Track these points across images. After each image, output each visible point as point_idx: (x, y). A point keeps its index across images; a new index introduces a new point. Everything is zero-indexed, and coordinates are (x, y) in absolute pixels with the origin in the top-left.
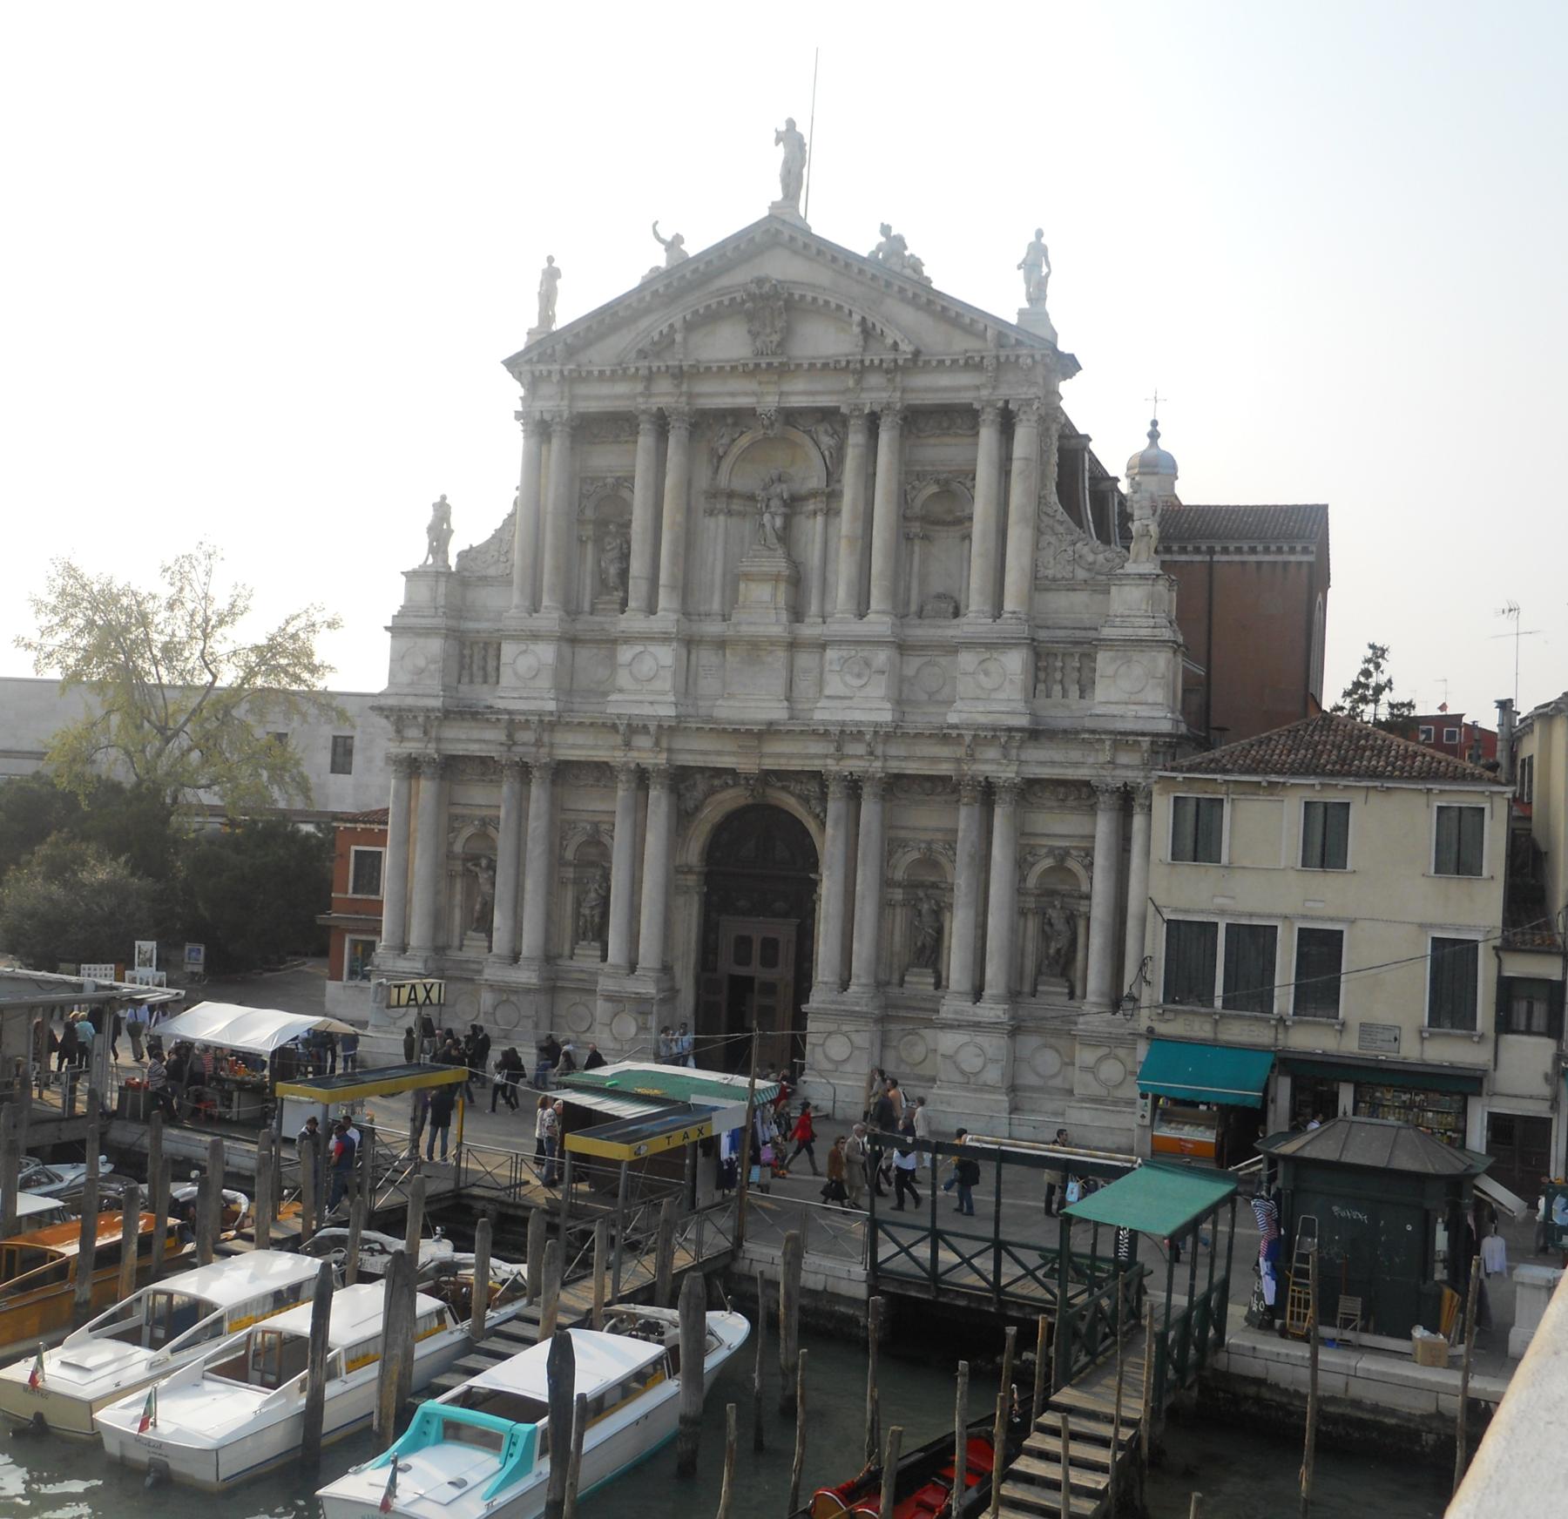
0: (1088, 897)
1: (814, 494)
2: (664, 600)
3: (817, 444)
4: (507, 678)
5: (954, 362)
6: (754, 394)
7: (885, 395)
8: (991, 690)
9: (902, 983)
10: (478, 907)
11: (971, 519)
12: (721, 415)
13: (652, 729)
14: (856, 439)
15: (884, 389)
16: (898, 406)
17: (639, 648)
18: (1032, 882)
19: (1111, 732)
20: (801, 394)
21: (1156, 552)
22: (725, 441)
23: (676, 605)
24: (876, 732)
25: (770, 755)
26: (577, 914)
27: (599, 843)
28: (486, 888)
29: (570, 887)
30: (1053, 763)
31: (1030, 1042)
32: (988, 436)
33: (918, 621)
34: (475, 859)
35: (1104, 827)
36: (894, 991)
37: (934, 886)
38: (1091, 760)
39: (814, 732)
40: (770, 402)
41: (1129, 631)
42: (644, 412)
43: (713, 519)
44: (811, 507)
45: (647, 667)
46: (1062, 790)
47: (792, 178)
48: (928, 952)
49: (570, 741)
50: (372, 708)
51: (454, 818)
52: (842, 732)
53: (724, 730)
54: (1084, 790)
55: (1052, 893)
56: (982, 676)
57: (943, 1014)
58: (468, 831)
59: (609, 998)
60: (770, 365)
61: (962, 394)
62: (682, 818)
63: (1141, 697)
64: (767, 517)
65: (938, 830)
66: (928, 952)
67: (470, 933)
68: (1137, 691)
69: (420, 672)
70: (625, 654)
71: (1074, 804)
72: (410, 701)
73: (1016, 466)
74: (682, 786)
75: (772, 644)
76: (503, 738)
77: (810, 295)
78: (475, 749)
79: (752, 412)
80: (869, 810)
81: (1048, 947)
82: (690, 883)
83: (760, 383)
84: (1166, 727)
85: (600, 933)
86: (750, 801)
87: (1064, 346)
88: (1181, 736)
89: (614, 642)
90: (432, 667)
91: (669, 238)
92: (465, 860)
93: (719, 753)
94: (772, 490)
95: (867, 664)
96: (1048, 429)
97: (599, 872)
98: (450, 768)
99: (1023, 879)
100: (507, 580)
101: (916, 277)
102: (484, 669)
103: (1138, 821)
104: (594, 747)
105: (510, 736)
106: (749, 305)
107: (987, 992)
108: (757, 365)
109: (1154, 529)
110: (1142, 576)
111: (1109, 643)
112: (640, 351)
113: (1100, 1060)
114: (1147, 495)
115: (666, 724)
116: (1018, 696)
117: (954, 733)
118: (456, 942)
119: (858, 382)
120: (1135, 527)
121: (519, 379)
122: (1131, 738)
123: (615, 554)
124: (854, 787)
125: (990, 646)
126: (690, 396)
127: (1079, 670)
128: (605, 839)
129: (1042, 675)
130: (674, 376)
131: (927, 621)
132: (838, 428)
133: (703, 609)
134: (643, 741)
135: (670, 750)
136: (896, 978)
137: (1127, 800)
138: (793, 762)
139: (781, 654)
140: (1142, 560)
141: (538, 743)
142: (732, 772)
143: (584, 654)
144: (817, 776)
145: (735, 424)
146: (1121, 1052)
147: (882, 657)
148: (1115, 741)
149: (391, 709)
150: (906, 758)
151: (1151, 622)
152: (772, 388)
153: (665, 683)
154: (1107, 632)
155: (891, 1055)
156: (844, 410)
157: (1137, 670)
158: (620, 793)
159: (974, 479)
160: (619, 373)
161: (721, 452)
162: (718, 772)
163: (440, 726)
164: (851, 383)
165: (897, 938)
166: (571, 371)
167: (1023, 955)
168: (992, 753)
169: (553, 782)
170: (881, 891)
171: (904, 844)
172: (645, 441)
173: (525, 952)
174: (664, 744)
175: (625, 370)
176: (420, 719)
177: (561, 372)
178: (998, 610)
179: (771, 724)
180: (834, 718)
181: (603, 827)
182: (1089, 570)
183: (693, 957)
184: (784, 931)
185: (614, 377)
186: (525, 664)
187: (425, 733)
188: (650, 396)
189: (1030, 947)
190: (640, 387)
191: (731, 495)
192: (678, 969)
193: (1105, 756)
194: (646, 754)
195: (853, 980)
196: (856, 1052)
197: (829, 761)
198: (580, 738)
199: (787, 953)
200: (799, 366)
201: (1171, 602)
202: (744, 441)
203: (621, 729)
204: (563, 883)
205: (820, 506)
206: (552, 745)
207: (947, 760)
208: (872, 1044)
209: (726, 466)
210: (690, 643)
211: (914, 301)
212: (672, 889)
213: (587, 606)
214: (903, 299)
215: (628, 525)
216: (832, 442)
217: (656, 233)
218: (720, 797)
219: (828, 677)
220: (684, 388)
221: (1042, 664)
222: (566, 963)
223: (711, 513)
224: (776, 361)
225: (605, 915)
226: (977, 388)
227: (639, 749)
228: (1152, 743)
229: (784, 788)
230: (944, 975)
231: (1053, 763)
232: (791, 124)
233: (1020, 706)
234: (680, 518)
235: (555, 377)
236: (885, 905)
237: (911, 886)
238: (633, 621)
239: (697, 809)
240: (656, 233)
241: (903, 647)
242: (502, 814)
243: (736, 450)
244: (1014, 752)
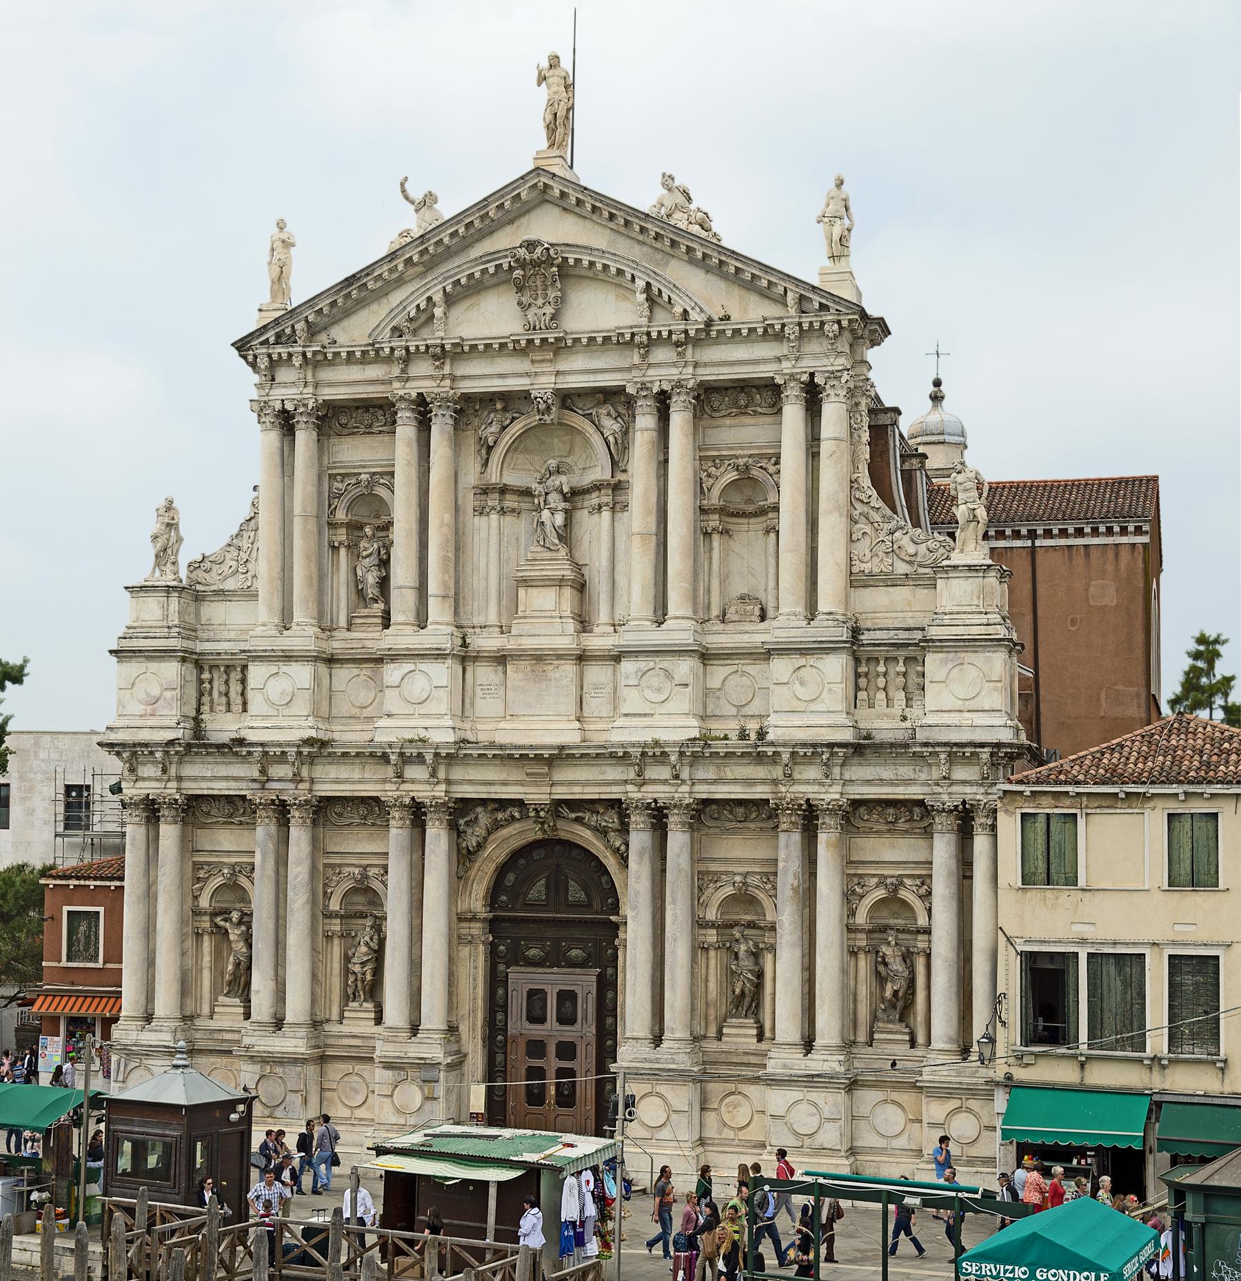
0: (927, 931)
1: (597, 487)
3: (598, 428)
4: (256, 702)
6: (528, 375)
7: (674, 371)
8: (808, 702)
9: (720, 1036)
10: (230, 967)
11: (776, 509)
12: (488, 400)
13: (429, 758)
14: (645, 421)
15: (674, 364)
16: (691, 384)
17: (407, 667)
18: (861, 918)
19: (946, 744)
20: (581, 372)
21: (986, 537)
22: (494, 428)
23: (448, 617)
24: (682, 754)
25: (562, 783)
26: (346, 972)
27: (369, 890)
28: (240, 946)
29: (336, 941)
30: (882, 782)
31: (868, 1098)
32: (793, 413)
33: (720, 627)
34: (225, 913)
35: (943, 849)
36: (711, 1046)
37: (752, 925)
38: (923, 776)
39: (613, 756)
40: (544, 383)
41: (955, 630)
42: (402, 398)
43: (485, 518)
44: (595, 502)
46: (891, 811)
47: (559, 125)
48: (747, 1000)
49: (332, 775)
50: (99, 744)
51: (197, 866)
52: (643, 754)
53: (510, 757)
54: (917, 810)
55: (884, 929)
57: (769, 1070)
58: (217, 881)
59: (388, 1066)
61: (761, 368)
62: (463, 857)
63: (972, 705)
64: (546, 514)
65: (754, 861)
66: (747, 1000)
67: (221, 999)
68: (970, 698)
70: (392, 673)
71: (906, 826)
73: (825, 448)
74: (462, 822)
75: (559, 657)
76: (256, 774)
78: (220, 788)
79: (525, 396)
80: (678, 840)
81: (883, 989)
82: (475, 932)
83: (533, 362)
84: (1006, 736)
85: (374, 990)
86: (540, 836)
87: (872, 311)
88: (1020, 746)
89: (379, 660)
90: (168, 694)
91: (418, 195)
92: (214, 914)
93: (505, 783)
94: (549, 482)
95: (669, 675)
96: (857, 404)
97: (369, 922)
98: (194, 809)
99: (852, 913)
100: (250, 595)
101: (703, 234)
102: (227, 695)
103: (981, 843)
105: (263, 771)
106: (518, 273)
107: (818, 1042)
108: (530, 342)
109: (982, 513)
110: (970, 568)
111: (940, 645)
112: (394, 329)
113: (951, 1114)
114: (973, 475)
115: (443, 752)
116: (841, 706)
117: (770, 750)
118: (206, 1010)
119: (644, 357)
120: (961, 512)
121: (253, 365)
122: (968, 750)
123: (374, 560)
124: (658, 816)
125: (803, 651)
126: (454, 378)
127: (905, 675)
128: (376, 885)
129: (863, 682)
130: (435, 357)
131: (730, 627)
132: (622, 410)
133: (477, 620)
134: (412, 772)
135: (448, 782)
136: (712, 1032)
137: (965, 818)
139: (569, 669)
140: (972, 551)
141: (297, 779)
142: (520, 803)
143: (343, 674)
144: (615, 804)
145: (505, 409)
146: (974, 1104)
148: (950, 754)
149: (123, 745)
150: (715, 782)
151: (983, 619)
152: (547, 367)
153: (442, 704)
154: (934, 632)
155: (711, 1117)
156: (631, 390)
157: (971, 673)
158: (393, 831)
159: (777, 463)
160: (371, 355)
161: (491, 441)
162: (503, 804)
163: (180, 763)
164: (636, 359)
165: (712, 985)
166: (315, 353)
167: (855, 1001)
168: (813, 772)
169: (314, 823)
170: (692, 933)
171: (716, 877)
172: (406, 431)
173: (289, 1018)
174: (442, 774)
175: (377, 351)
177: (304, 354)
178: (812, 610)
179: (562, 748)
180: (634, 739)
181: (372, 872)
182: (910, 563)
183: (480, 1015)
184: (585, 983)
185: (364, 360)
187: (164, 771)
188: (408, 380)
189: (863, 991)
190: (396, 371)
191: (504, 490)
192: (464, 1028)
193: (936, 774)
194: (420, 785)
195: (667, 1035)
196: (674, 1117)
197: (630, 788)
198: (342, 771)
199: (587, 1006)
200: (577, 341)
201: (1002, 596)
202: (516, 429)
203: (393, 758)
204: (329, 938)
205: (605, 499)
206: (312, 781)
207: (764, 782)
208: (691, 1104)
210: (465, 657)
211: (703, 263)
212: (455, 940)
213: (343, 622)
214: (692, 261)
215: (388, 526)
216: (616, 427)
218: (505, 832)
219: (624, 692)
220: (447, 370)
221: (863, 669)
222: (333, 1028)
223: (481, 511)
224: (551, 337)
225: (378, 971)
226: (779, 360)
227: (413, 781)
228: (992, 755)
229: (579, 820)
230: (767, 1026)
231: (882, 782)
232: (554, 62)
233: (842, 719)
234: (448, 518)
235: (297, 361)
236: (699, 949)
237: (725, 926)
238: (401, 636)
239: (480, 846)
240: (403, 191)
241: (706, 656)
242: (258, 860)
243: (507, 439)
244: (836, 770)
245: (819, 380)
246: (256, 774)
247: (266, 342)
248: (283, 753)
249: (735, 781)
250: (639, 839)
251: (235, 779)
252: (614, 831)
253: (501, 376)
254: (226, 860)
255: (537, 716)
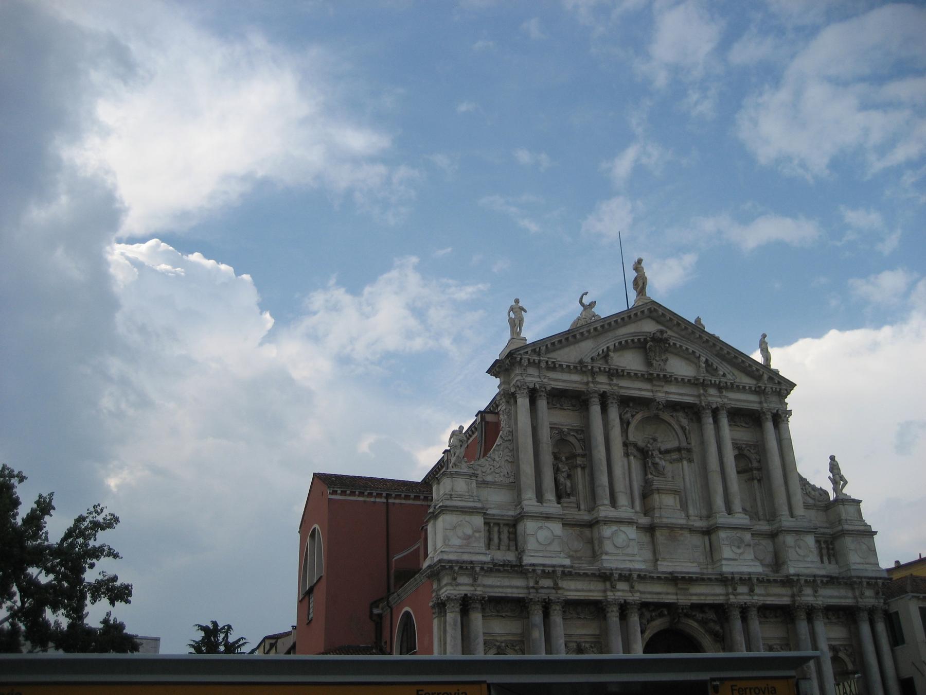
2: (623, 500)
3: (678, 422)
5: (750, 388)
6: (652, 391)
17: (614, 528)
20: (675, 393)
42: (596, 392)
45: (620, 539)
56: (797, 549)
60: (665, 376)
69: (468, 538)
70: (607, 531)
72: (466, 557)
77: (678, 344)
90: (477, 535)
93: (668, 594)
95: (741, 540)
104: (590, 591)
108: (658, 375)
122: (874, 581)
138: (708, 598)
139: (686, 534)
147: (747, 537)
148: (868, 583)
160: (580, 367)
176: (478, 569)
177: (547, 362)
186: (543, 535)
198: (579, 585)
202: (639, 417)
209: (631, 428)
217: (581, 299)
235: (543, 365)
240: (581, 299)
245: (780, 412)
246: (531, 584)
247: (527, 352)
248: (553, 571)
249: (775, 595)
250: (738, 625)
251: (517, 587)
252: (714, 621)
253: (640, 390)
254: (499, 639)
255: (684, 559)
